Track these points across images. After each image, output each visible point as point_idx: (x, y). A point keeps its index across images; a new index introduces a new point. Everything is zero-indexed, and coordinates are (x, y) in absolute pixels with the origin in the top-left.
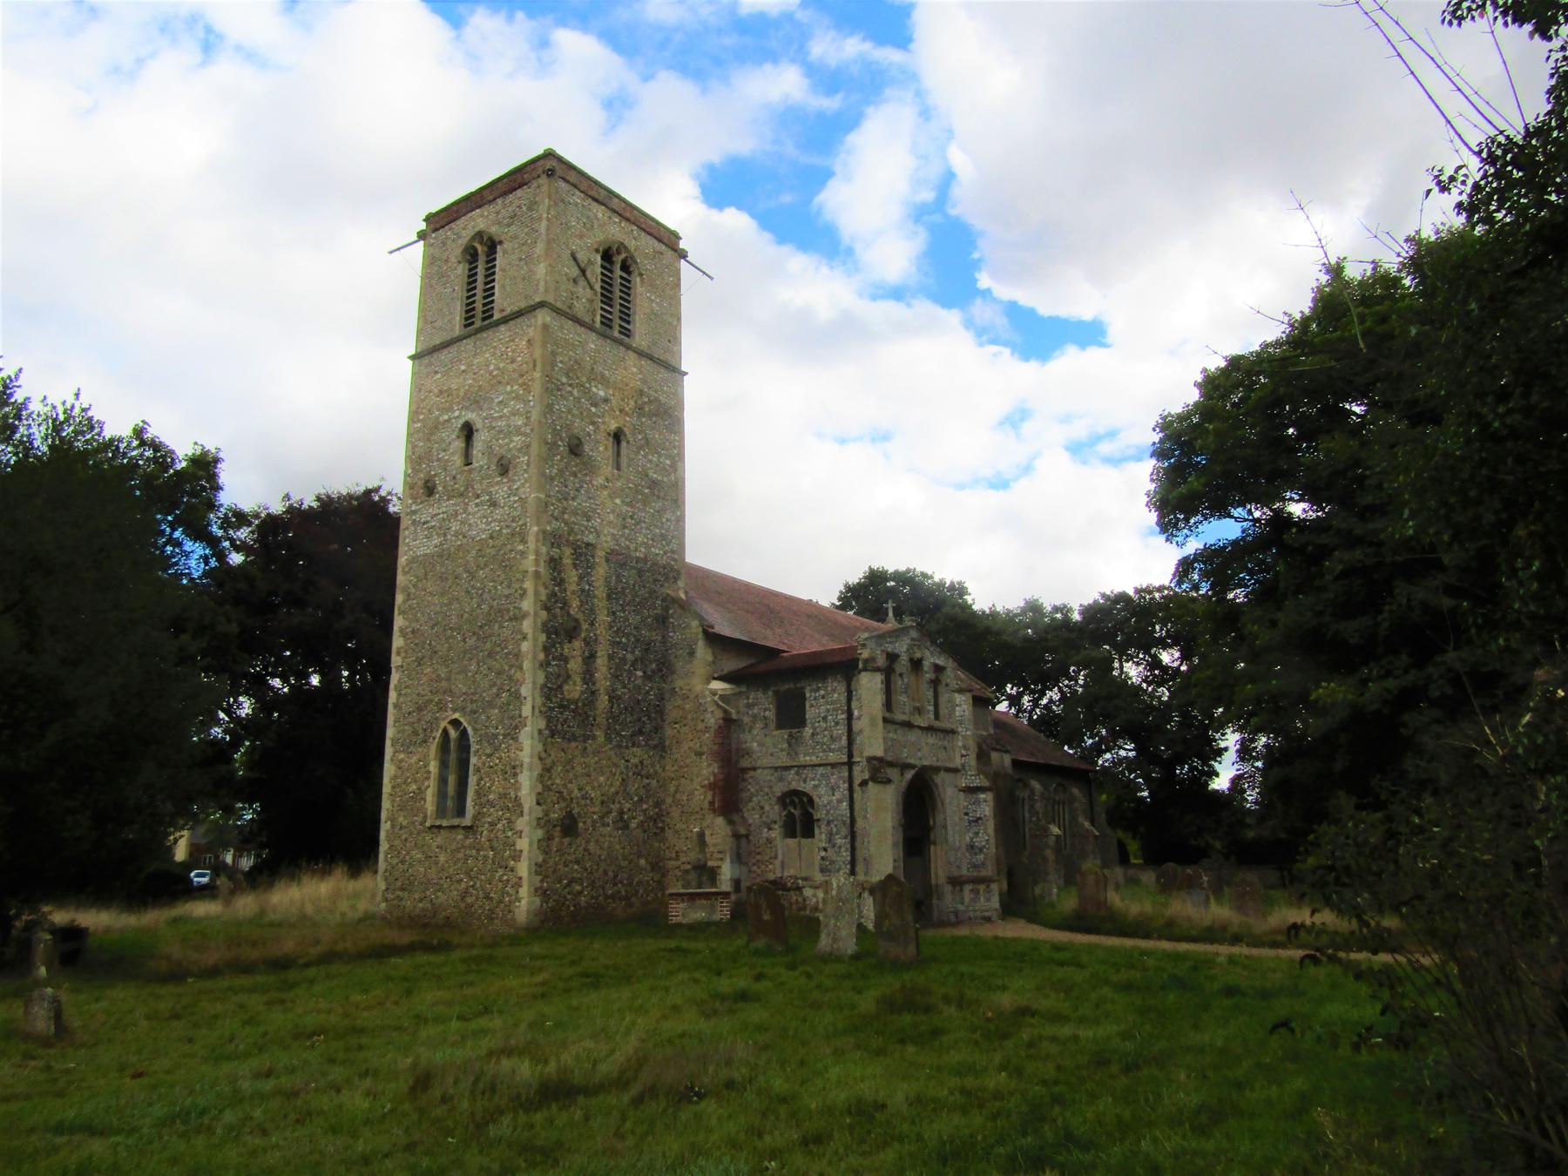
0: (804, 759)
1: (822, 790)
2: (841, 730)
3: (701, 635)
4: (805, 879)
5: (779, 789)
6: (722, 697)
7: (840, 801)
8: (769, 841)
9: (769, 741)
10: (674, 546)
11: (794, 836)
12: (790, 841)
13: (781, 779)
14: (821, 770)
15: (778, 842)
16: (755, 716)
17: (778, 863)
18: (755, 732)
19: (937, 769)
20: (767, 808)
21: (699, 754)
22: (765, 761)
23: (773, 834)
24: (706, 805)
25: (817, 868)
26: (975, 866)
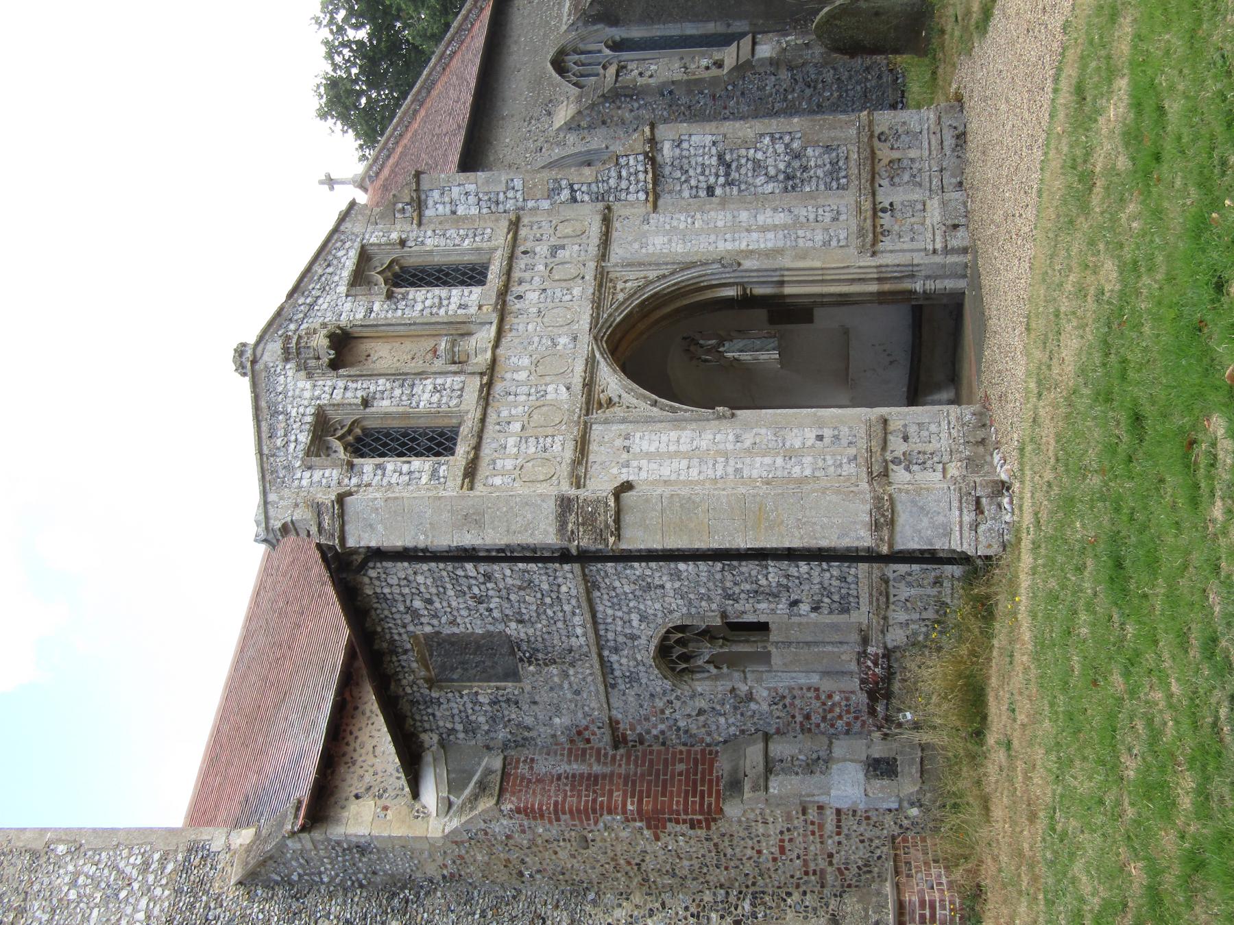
0: (581, 636)
1: (652, 606)
2: (501, 571)
3: (317, 835)
4: (865, 641)
5: (655, 681)
6: (455, 786)
7: (677, 575)
8: (778, 699)
9: (543, 696)
10: (130, 864)
11: (765, 658)
12: (776, 660)
13: (632, 679)
14: (604, 609)
15: (782, 682)
16: (493, 720)
17: (827, 685)
18: (529, 721)
19: (603, 279)
20: (702, 703)
21: (585, 843)
22: (594, 703)
23: (762, 693)
24: (701, 833)
25: (843, 618)
26: (834, 171)
